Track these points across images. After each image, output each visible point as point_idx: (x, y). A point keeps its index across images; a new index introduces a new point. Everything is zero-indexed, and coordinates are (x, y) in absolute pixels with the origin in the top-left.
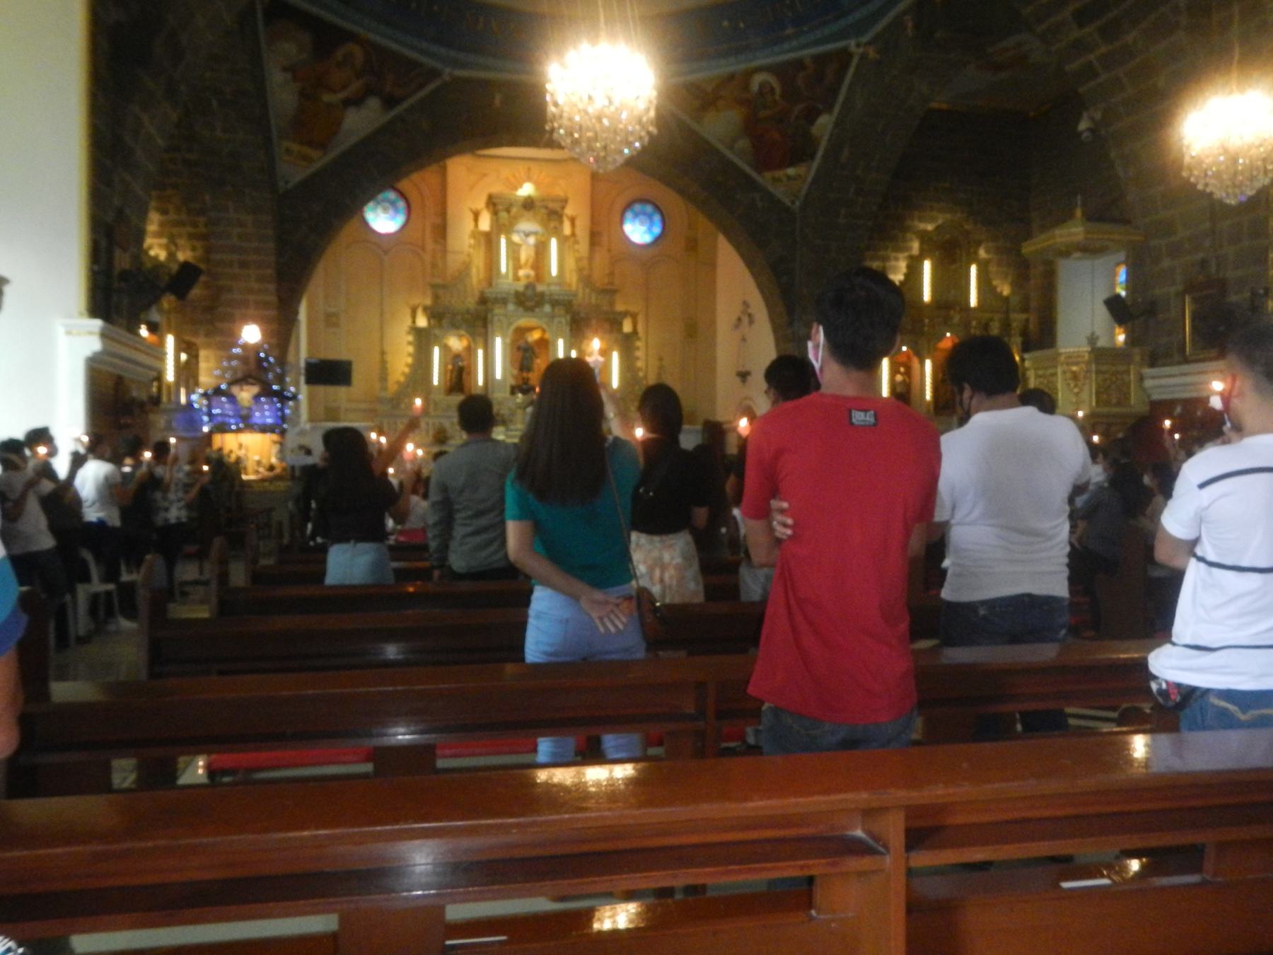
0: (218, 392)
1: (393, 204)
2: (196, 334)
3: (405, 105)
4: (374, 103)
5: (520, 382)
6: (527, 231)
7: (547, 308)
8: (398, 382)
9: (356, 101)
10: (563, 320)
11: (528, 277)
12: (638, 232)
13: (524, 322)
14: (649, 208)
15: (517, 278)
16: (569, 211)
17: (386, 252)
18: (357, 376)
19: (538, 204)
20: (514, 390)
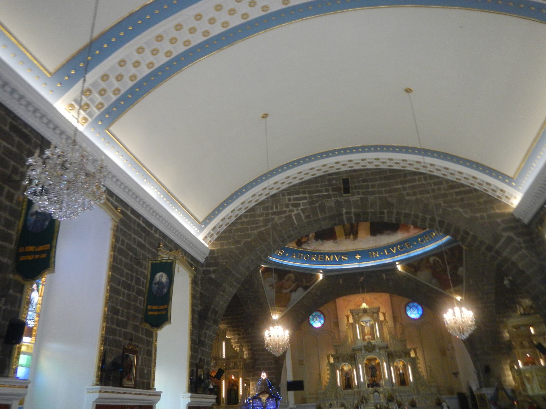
0: (254, 398)
1: (319, 316)
2: (249, 376)
3: (311, 288)
4: (300, 289)
5: (372, 382)
6: (366, 321)
7: (377, 350)
8: (325, 386)
9: (294, 290)
10: (384, 355)
11: (369, 339)
12: (414, 314)
13: (371, 356)
14: (416, 304)
15: (364, 339)
16: (382, 310)
17: (318, 335)
18: (306, 385)
19: (368, 311)
20: (369, 386)
